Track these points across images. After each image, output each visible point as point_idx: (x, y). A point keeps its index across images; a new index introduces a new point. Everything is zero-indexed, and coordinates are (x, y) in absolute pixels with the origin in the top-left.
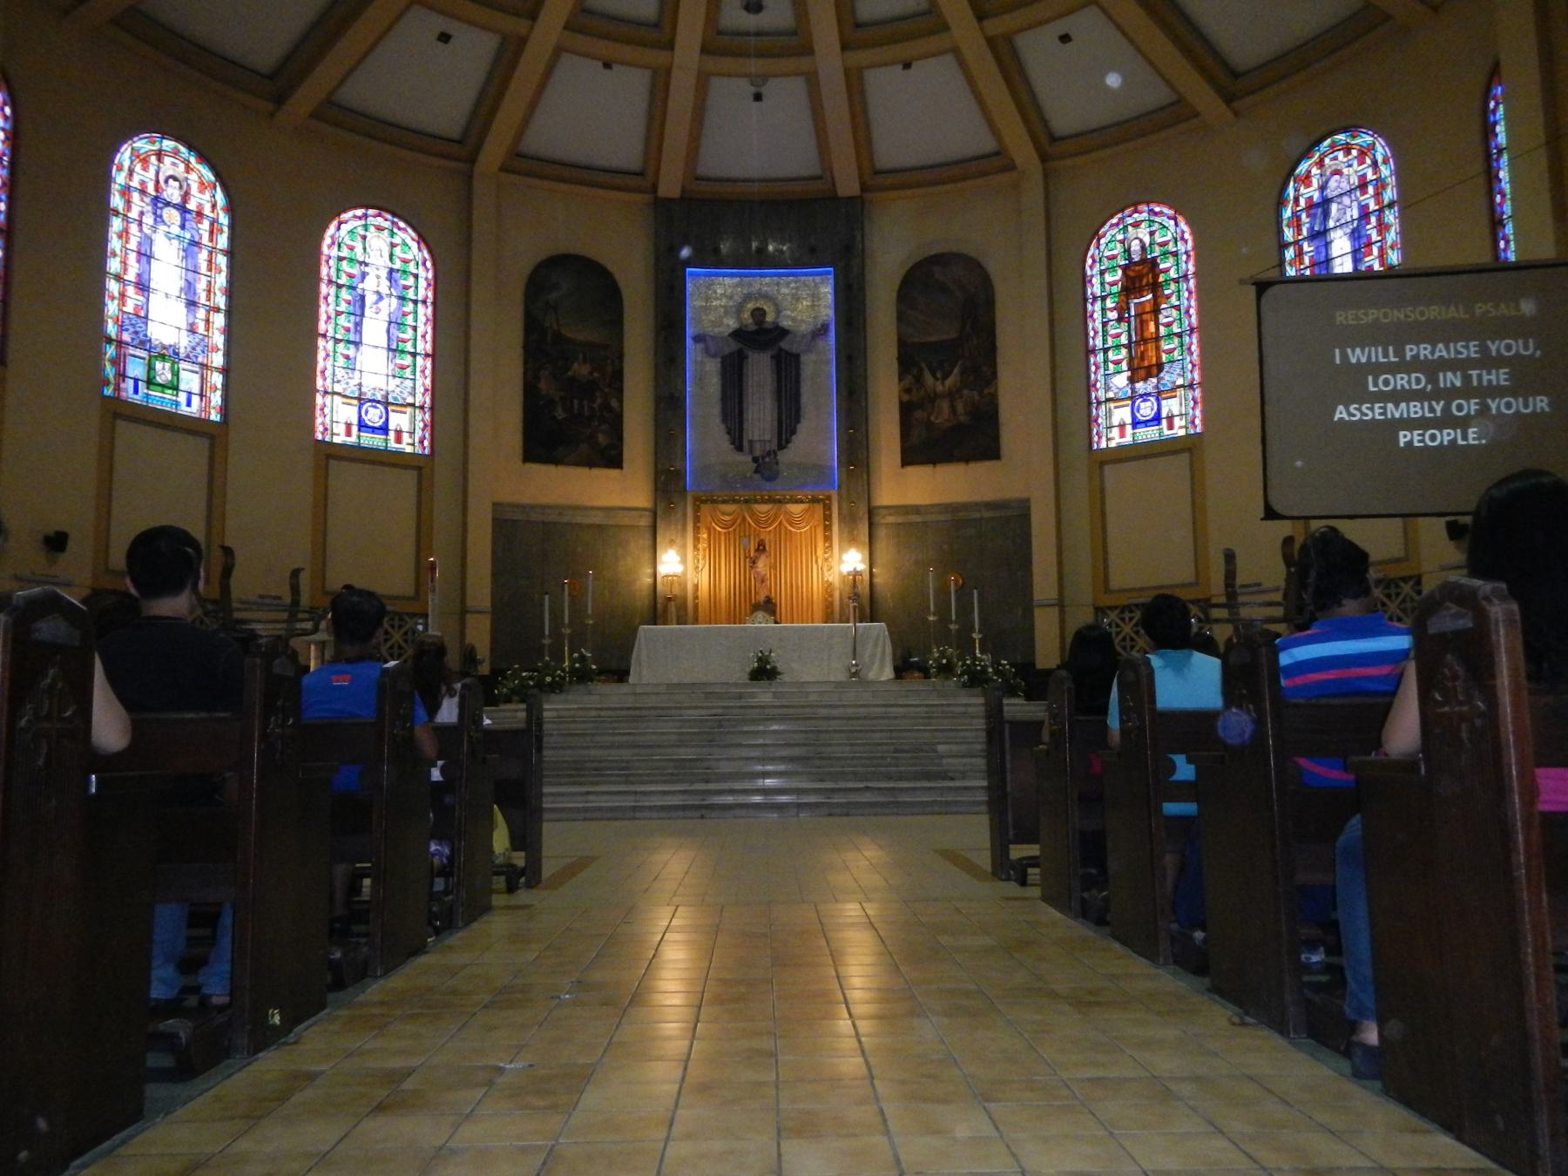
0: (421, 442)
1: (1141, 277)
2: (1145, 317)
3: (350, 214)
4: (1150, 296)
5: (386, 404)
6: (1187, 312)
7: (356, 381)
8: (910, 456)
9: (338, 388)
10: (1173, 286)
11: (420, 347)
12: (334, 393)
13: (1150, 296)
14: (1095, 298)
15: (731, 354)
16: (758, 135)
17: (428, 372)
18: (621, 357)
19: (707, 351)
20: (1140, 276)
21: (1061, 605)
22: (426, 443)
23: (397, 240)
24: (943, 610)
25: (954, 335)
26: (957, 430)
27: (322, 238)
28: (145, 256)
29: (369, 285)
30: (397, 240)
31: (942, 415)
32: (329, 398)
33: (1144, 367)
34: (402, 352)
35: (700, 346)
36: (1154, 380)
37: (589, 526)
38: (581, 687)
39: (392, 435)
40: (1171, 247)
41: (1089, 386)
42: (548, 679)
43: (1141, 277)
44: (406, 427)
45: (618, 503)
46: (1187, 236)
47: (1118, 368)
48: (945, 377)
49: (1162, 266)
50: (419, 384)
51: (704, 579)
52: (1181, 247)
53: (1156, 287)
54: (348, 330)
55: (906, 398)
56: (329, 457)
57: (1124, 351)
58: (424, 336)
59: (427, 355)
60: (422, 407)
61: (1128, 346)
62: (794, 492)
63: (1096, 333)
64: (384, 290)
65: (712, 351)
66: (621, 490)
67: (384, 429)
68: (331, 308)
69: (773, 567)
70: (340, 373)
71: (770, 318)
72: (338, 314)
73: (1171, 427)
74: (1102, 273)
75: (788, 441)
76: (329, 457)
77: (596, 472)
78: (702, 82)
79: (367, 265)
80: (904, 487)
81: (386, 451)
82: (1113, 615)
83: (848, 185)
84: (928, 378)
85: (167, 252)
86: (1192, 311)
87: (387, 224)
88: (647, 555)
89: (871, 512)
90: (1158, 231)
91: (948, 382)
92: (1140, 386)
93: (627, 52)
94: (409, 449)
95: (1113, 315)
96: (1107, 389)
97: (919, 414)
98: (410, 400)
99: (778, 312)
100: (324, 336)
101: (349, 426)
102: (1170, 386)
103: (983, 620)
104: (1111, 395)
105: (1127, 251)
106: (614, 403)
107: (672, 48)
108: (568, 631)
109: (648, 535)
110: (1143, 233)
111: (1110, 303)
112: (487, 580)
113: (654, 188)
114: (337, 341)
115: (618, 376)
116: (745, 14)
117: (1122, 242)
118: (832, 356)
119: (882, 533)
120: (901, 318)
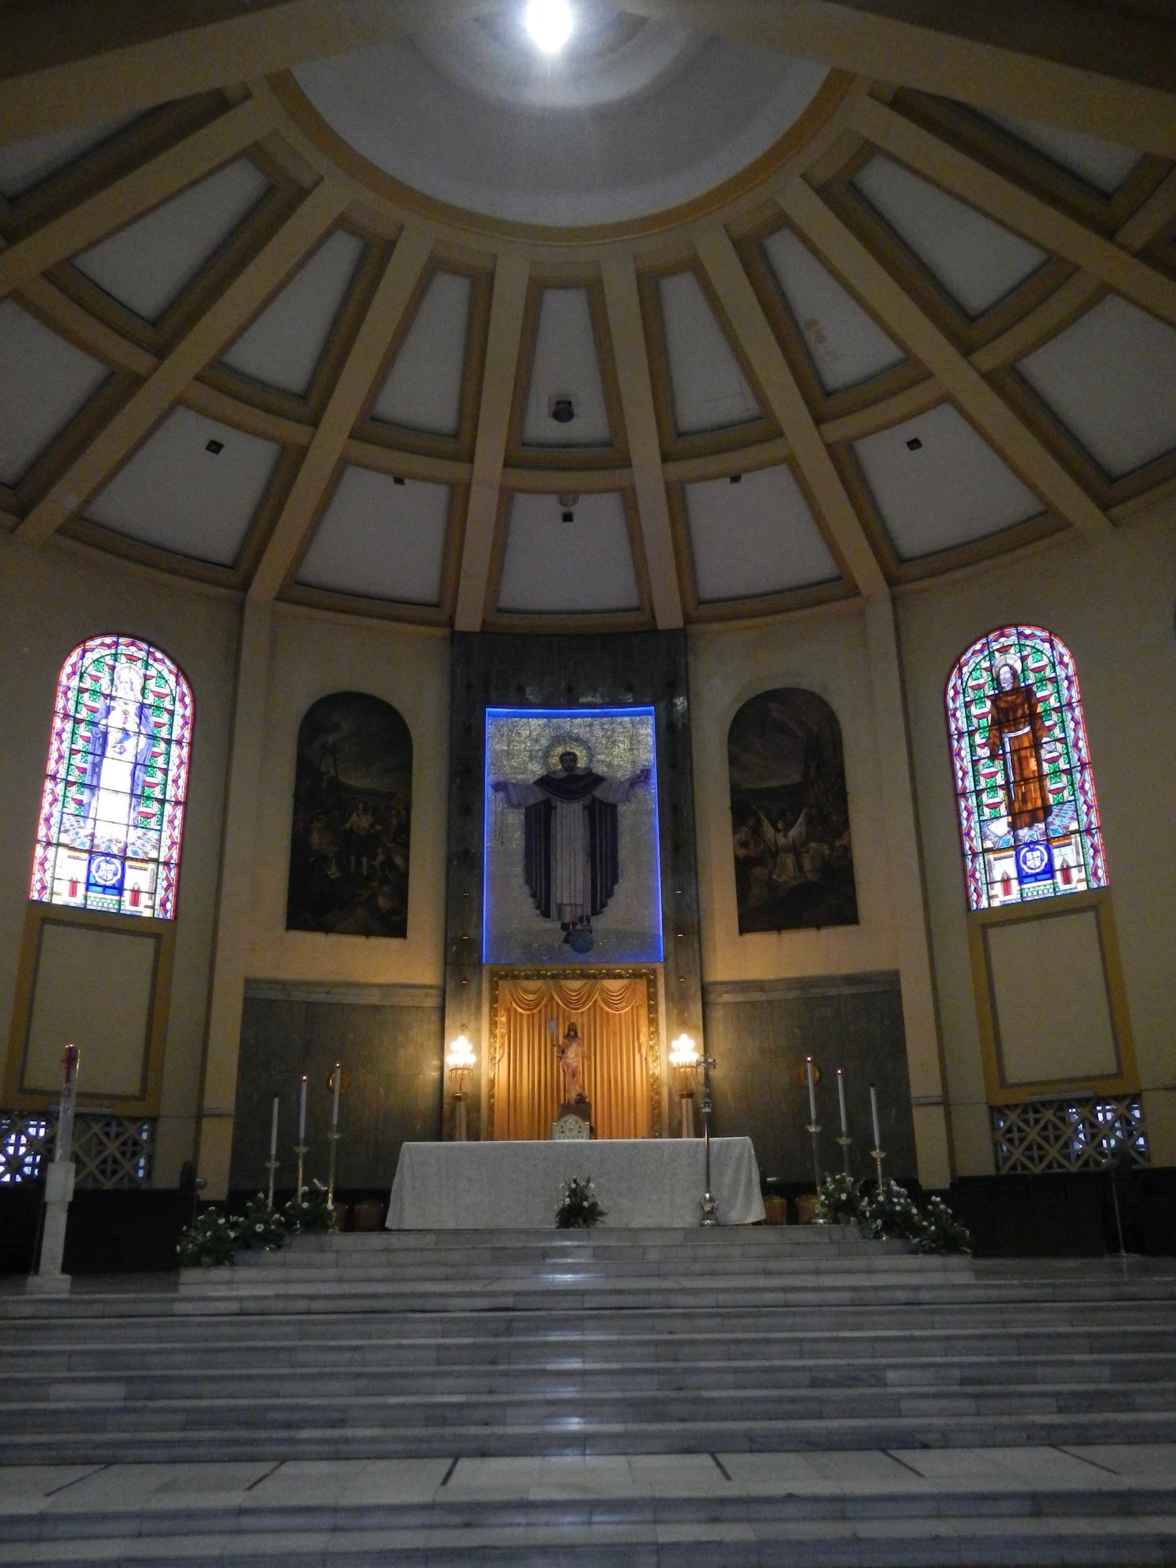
0: (163, 905)
1: (1015, 708)
2: (1023, 753)
3: (98, 641)
4: (1027, 729)
5: (124, 858)
6: (1076, 745)
7: (89, 831)
8: (749, 923)
9: (64, 839)
10: (1055, 717)
11: (170, 793)
12: (59, 845)
13: (1027, 729)
14: (961, 734)
15: (538, 804)
16: (569, 563)
17: (177, 822)
18: (408, 807)
19: (509, 803)
20: (1013, 708)
21: (945, 1102)
22: (169, 906)
23: (152, 672)
24: (828, 1116)
25: (792, 776)
26: (804, 889)
27: (61, 667)
29: (115, 720)
30: (152, 672)
31: (787, 872)
32: (51, 851)
33: (1027, 809)
34: (148, 798)
35: (501, 795)
36: (1042, 826)
37: (365, 1008)
38: (311, 1239)
39: (127, 896)
40: (1049, 673)
41: (961, 835)
42: (260, 1228)
43: (1015, 708)
44: (145, 886)
46: (1066, 659)
47: (995, 813)
48: (788, 828)
49: (1039, 695)
50: (165, 840)
51: (502, 1073)
52: (1061, 672)
53: (1034, 719)
54: (83, 771)
55: (742, 853)
56: (45, 920)
57: (1001, 794)
58: (175, 781)
59: (177, 803)
60: (167, 864)
61: (1006, 787)
62: (612, 966)
63: (965, 773)
64: (132, 726)
65: (515, 802)
66: (404, 963)
67: (119, 889)
68: (64, 745)
69: (586, 1057)
70: (68, 821)
71: (581, 764)
72: (73, 752)
73: (1067, 880)
74: (967, 705)
75: (604, 905)
76: (45, 920)
77: (374, 941)
78: (506, 496)
79: (112, 698)
80: (745, 958)
81: (119, 915)
82: (1013, 1117)
83: (669, 616)
84: (769, 831)
86: (1081, 744)
87: (142, 655)
88: (432, 1043)
89: (704, 990)
90: (1030, 655)
91: (794, 832)
92: (1025, 834)
93: (418, 464)
94: (147, 913)
95: (985, 752)
96: (983, 837)
97: (758, 872)
98: (153, 854)
99: (591, 756)
100: (54, 777)
101: (74, 884)
102: (1061, 832)
103: (849, 1121)
104: (989, 844)
105: (996, 680)
106: (398, 861)
107: (471, 460)
108: (302, 1150)
109: (435, 1018)
110: (1013, 659)
111: (979, 739)
112: (233, 1073)
113: (451, 620)
114: (69, 784)
115: (405, 828)
116: (553, 423)
117: (989, 669)
118: (654, 806)
119: (718, 1014)
120: (733, 761)
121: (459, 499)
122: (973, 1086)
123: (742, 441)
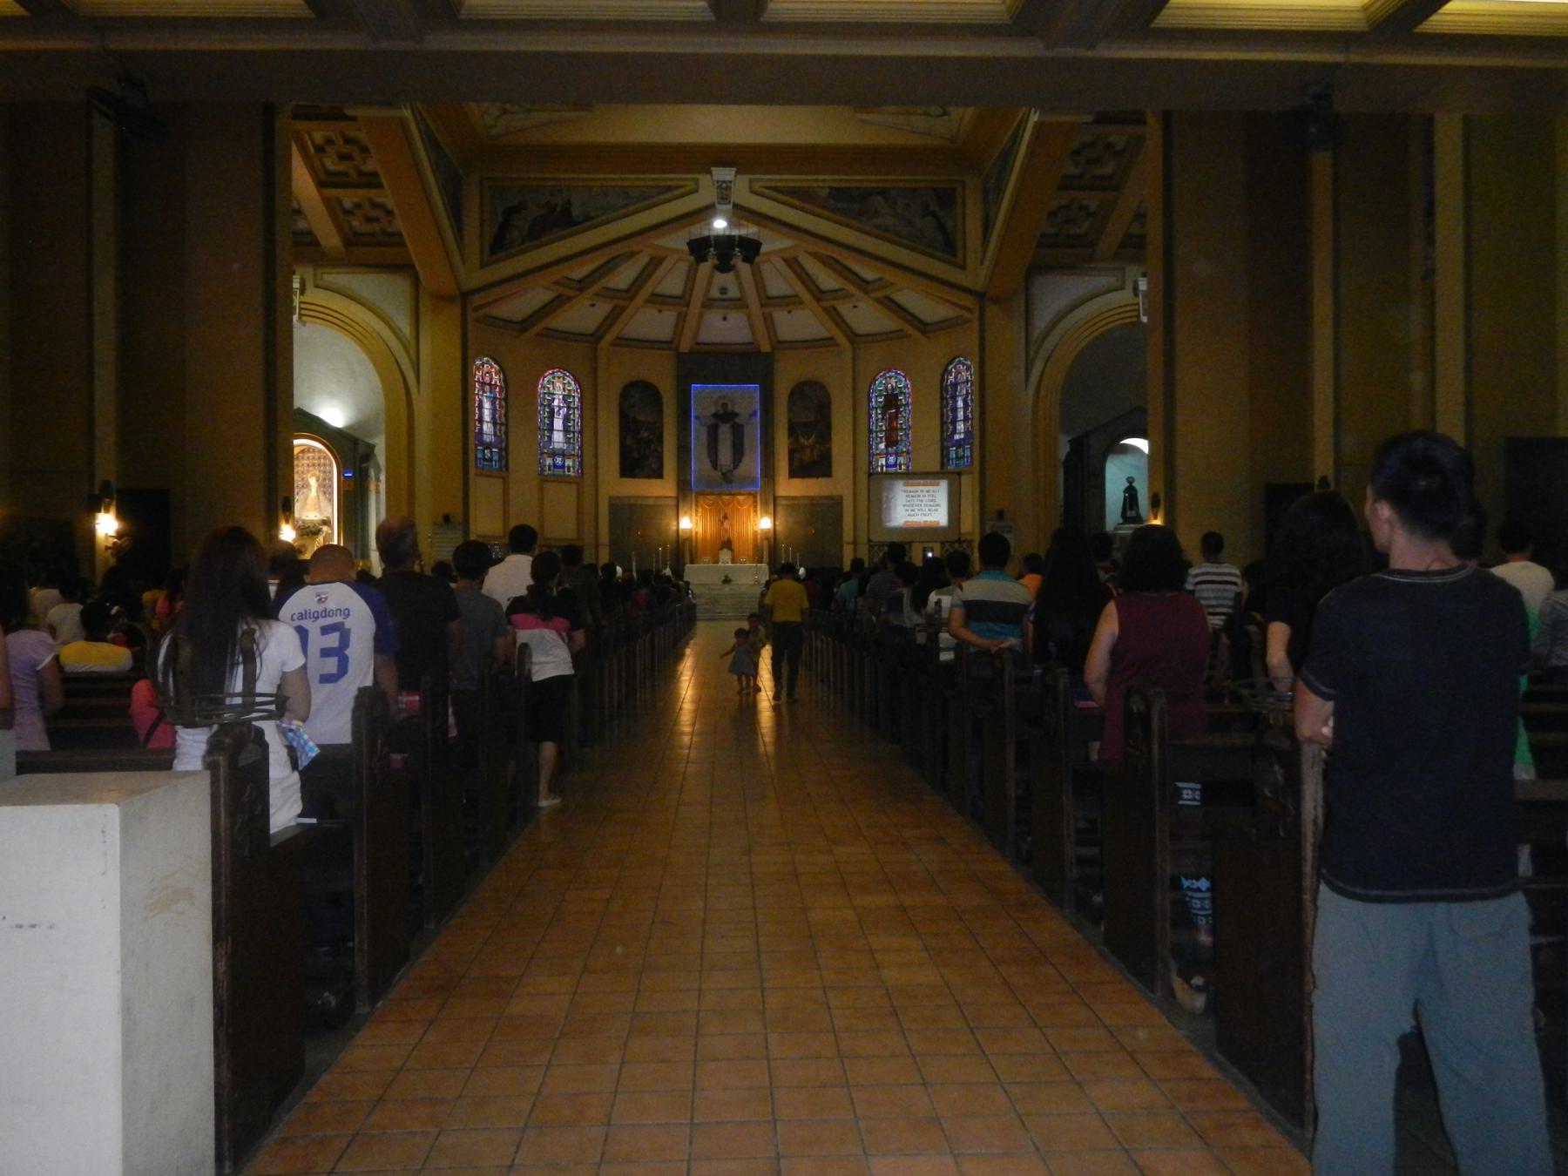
8: (794, 473)
16: (725, 329)
26: (813, 464)
28: (481, 407)
29: (556, 403)
31: (807, 456)
33: (891, 442)
43: (892, 400)
45: (661, 494)
51: (700, 530)
53: (897, 407)
66: (664, 488)
67: (563, 467)
80: (790, 487)
83: (765, 347)
84: (802, 440)
85: (487, 405)
89: (775, 499)
110: (893, 381)
119: (780, 509)
120: (790, 410)
121: (681, 319)
122: (863, 538)
123: (789, 302)
